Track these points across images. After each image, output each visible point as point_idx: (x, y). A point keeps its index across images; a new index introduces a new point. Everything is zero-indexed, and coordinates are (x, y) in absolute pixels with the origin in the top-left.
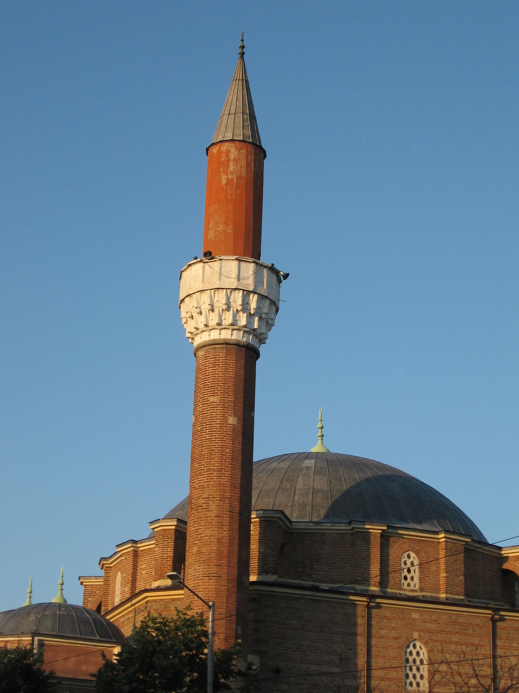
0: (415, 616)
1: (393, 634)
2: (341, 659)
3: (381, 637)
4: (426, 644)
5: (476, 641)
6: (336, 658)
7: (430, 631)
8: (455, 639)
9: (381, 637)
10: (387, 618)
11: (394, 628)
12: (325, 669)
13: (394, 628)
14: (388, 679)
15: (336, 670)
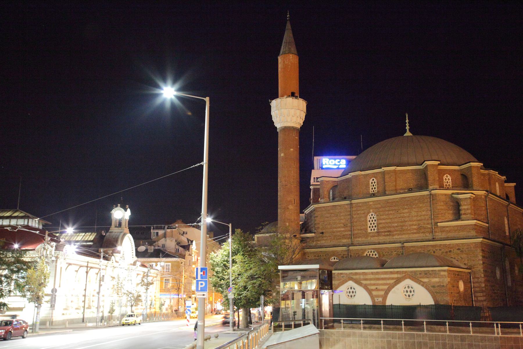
0: (371, 203)
1: (363, 212)
3: (358, 214)
4: (375, 213)
6: (342, 225)
8: (387, 209)
9: (358, 214)
10: (360, 206)
11: (363, 210)
12: (339, 230)
13: (363, 210)
14: (361, 230)
15: (342, 229)
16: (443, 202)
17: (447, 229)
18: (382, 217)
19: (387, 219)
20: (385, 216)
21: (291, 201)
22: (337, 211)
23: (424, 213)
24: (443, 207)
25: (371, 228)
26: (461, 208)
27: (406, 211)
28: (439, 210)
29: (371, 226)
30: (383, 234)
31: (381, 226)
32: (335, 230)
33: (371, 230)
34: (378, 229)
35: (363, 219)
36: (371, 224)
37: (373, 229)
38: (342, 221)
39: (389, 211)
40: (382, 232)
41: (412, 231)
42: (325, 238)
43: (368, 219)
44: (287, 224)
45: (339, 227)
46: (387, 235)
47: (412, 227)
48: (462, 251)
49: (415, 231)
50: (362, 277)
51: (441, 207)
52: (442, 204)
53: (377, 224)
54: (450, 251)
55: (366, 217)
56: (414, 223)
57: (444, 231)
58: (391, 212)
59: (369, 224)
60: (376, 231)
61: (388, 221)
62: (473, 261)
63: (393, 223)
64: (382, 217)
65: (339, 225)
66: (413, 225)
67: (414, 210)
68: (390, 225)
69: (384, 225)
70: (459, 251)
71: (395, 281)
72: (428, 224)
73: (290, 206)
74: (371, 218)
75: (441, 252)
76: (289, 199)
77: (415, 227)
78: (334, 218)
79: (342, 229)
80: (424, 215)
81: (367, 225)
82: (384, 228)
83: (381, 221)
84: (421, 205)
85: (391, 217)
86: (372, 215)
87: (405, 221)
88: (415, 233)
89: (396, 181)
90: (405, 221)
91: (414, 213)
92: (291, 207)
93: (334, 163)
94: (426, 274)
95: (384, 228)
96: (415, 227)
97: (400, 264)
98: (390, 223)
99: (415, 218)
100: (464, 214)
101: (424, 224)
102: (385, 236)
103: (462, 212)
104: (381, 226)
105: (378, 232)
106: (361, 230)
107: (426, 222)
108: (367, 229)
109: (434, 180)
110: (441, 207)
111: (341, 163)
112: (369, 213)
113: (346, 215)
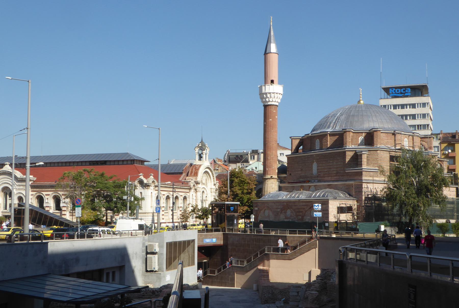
23: (339, 163)
27: (331, 161)
49: (335, 175)
55: (312, 165)
56: (335, 169)
61: (323, 168)
66: (333, 171)
87: (330, 168)
90: (330, 168)
93: (399, 92)
99: (335, 167)
111: (407, 91)
112: (313, 162)
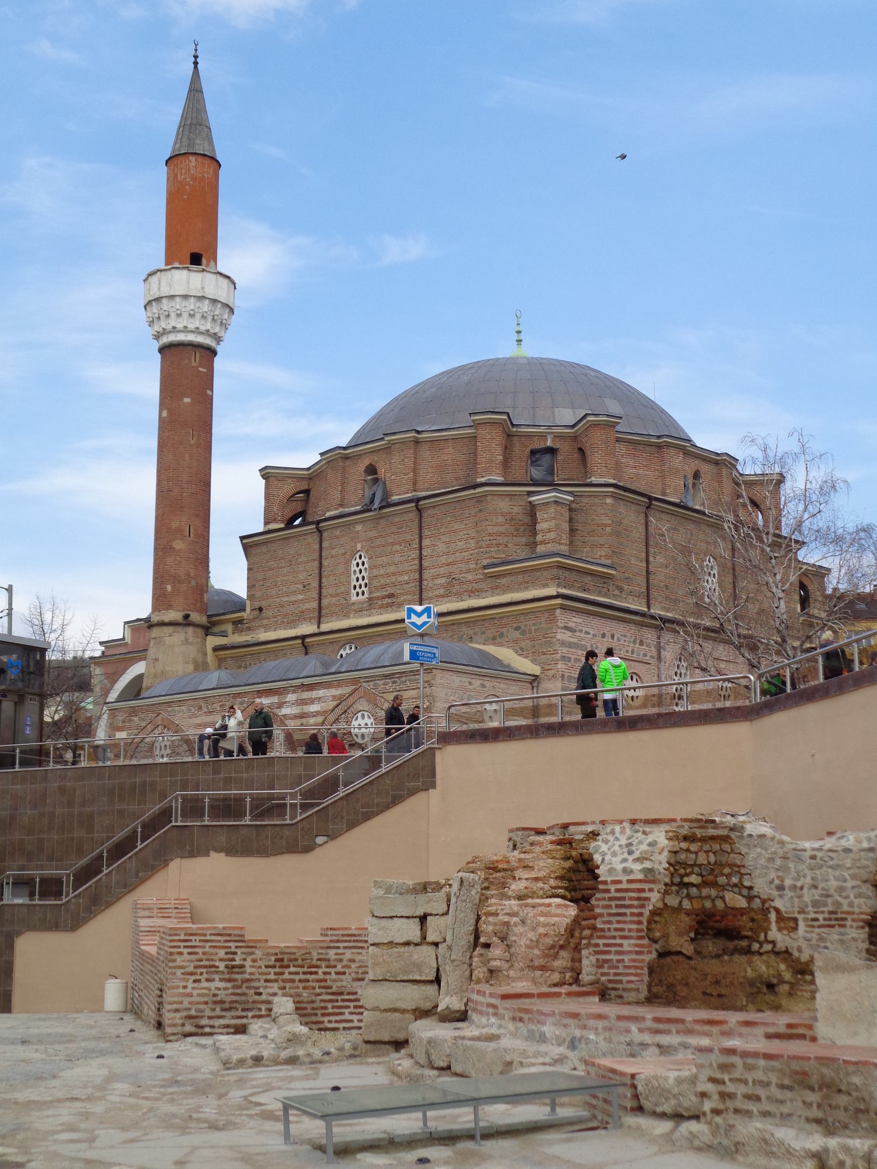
1: (343, 551)
2: (304, 587)
4: (366, 552)
5: (408, 537)
6: (300, 586)
7: (370, 539)
8: (391, 541)
10: (336, 537)
11: (342, 546)
13: (342, 546)
14: (337, 595)
15: (300, 597)
16: (503, 515)
17: (504, 581)
18: (379, 561)
19: (389, 564)
20: (384, 558)
21: (179, 531)
22: (292, 551)
24: (502, 529)
25: (358, 589)
26: (538, 527)
28: (490, 535)
29: (357, 584)
30: (380, 602)
31: (375, 583)
32: (286, 599)
33: (358, 594)
34: (370, 592)
35: (341, 569)
36: (358, 580)
37: (360, 591)
38: (301, 577)
39: (393, 544)
40: (378, 598)
41: (437, 593)
42: (265, 622)
43: (354, 568)
44: (169, 588)
45: (294, 592)
46: (388, 605)
47: (436, 581)
48: (523, 633)
49: (442, 591)
50: (275, 699)
51: (496, 529)
52: (501, 519)
53: (370, 579)
54: (502, 635)
55: (348, 563)
56: (442, 571)
57: (497, 587)
58: (397, 547)
59: (354, 577)
60: (366, 595)
61: (392, 569)
62: (544, 654)
63: (400, 573)
64: (379, 561)
65: (293, 588)
67: (444, 538)
68: (393, 579)
69: (383, 581)
70: (516, 634)
71: (335, 703)
72: (468, 571)
73: (180, 542)
74: (358, 565)
75: (485, 636)
76: (175, 524)
77: (442, 581)
78: (285, 570)
79: (300, 597)
80: (461, 550)
81: (349, 582)
82: (383, 587)
83: (376, 572)
84: (456, 526)
85: (397, 558)
86: (360, 557)
88: (442, 596)
89: (415, 470)
91: (442, 547)
92: (179, 545)
94: (394, 682)
95: (383, 587)
96: (442, 581)
97: (526, 701)
98: (394, 574)
99: (443, 560)
100: (542, 543)
101: (461, 572)
102: (381, 607)
103: (539, 538)
104: (375, 583)
105: (370, 599)
106: (337, 595)
107: (464, 567)
108: (348, 593)
109: (491, 461)
110: (496, 529)
113: (308, 562)
